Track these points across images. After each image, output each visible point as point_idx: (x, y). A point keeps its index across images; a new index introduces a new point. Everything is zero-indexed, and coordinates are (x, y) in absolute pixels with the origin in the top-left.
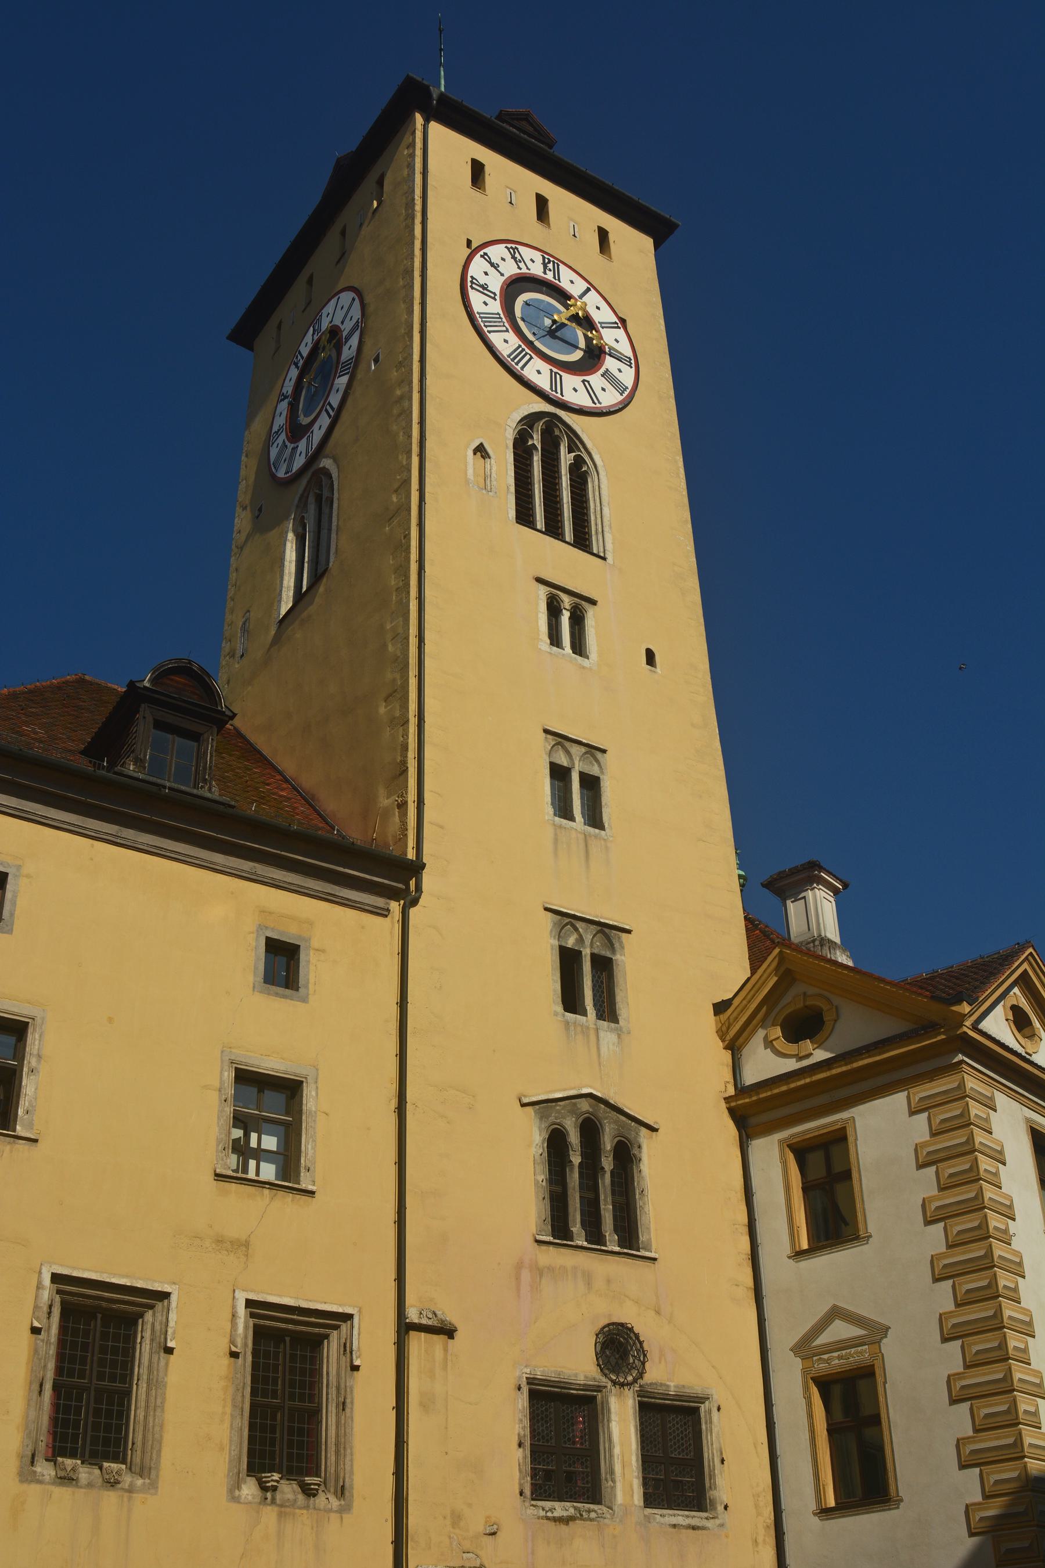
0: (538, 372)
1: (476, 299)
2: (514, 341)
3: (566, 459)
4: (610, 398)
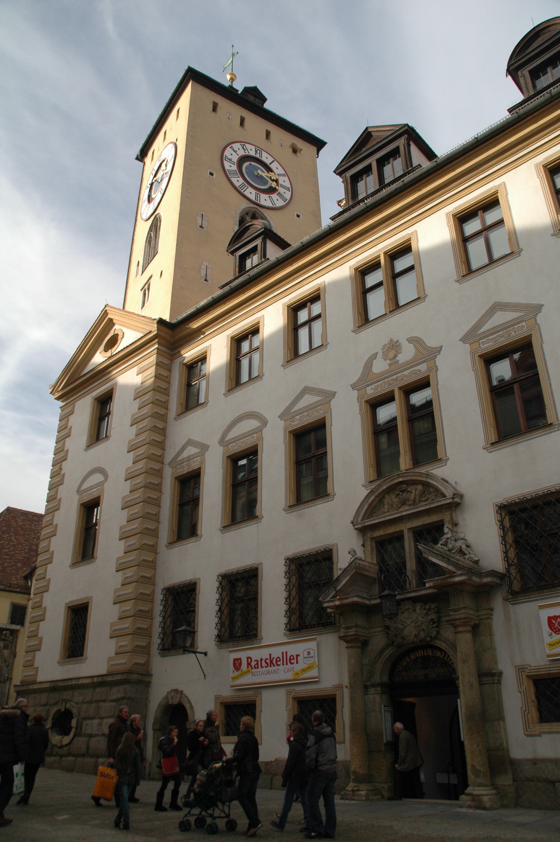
0: (250, 193)
1: (227, 165)
2: (241, 181)
4: (280, 203)
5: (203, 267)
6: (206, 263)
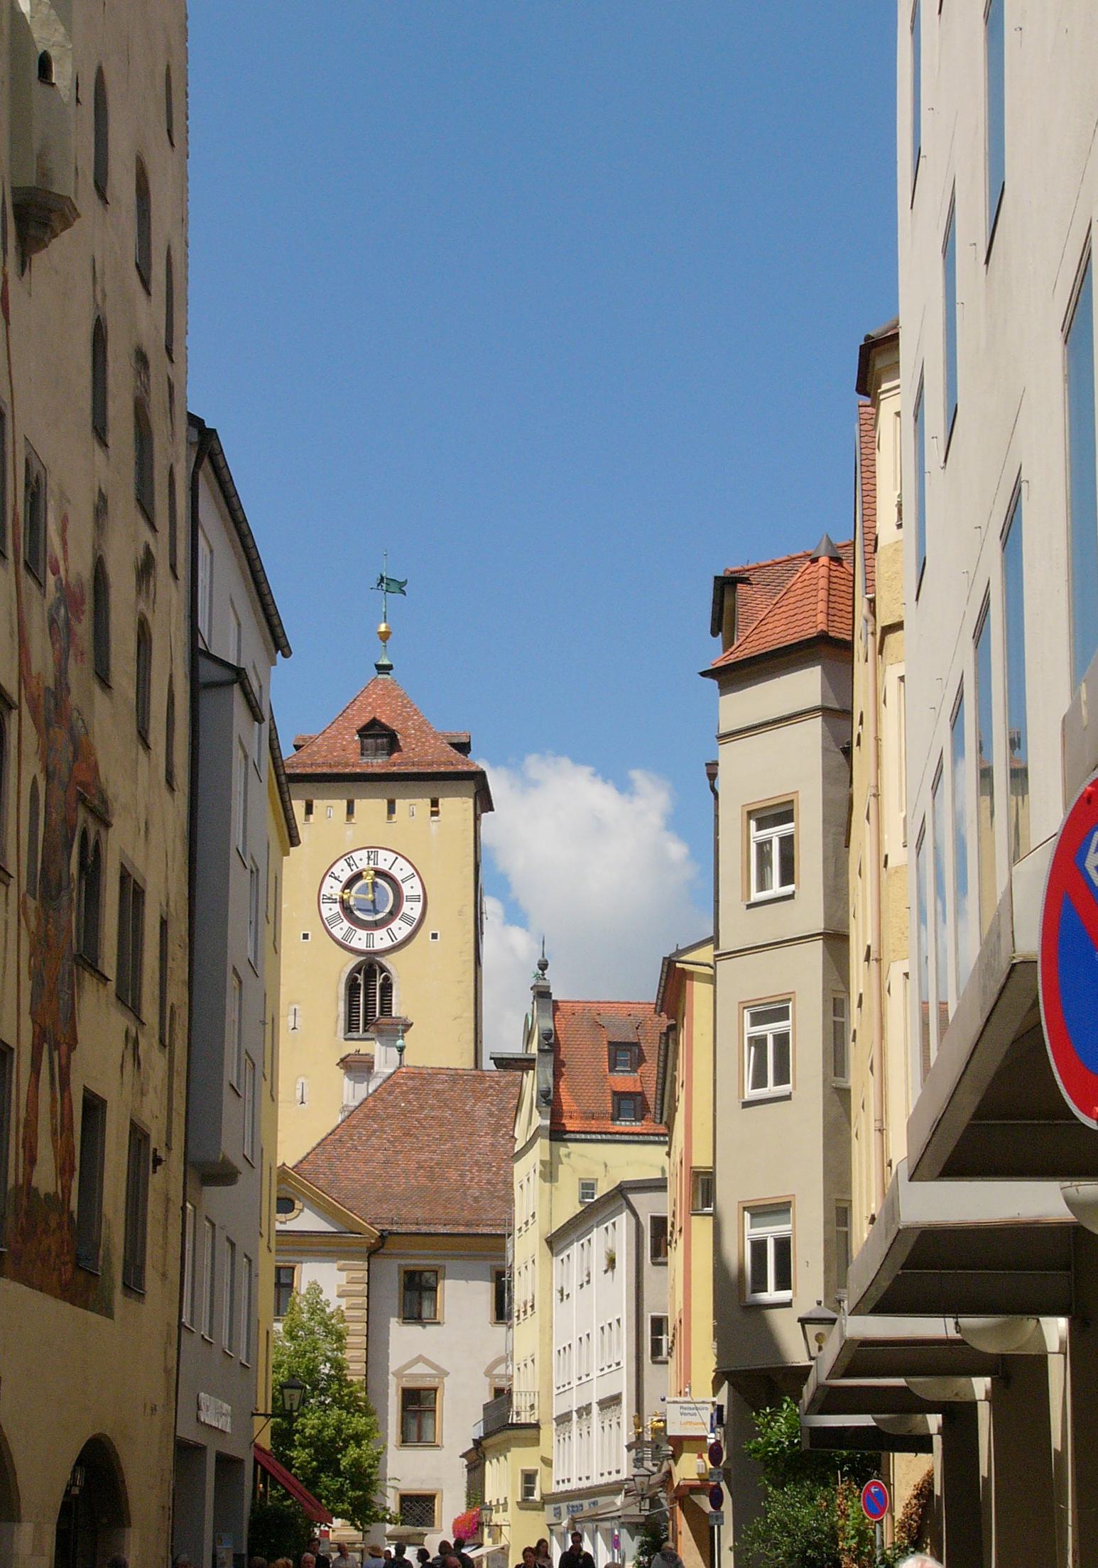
0: (360, 940)
2: (346, 924)
3: (379, 981)
5: (299, 1086)
6: (301, 1080)
